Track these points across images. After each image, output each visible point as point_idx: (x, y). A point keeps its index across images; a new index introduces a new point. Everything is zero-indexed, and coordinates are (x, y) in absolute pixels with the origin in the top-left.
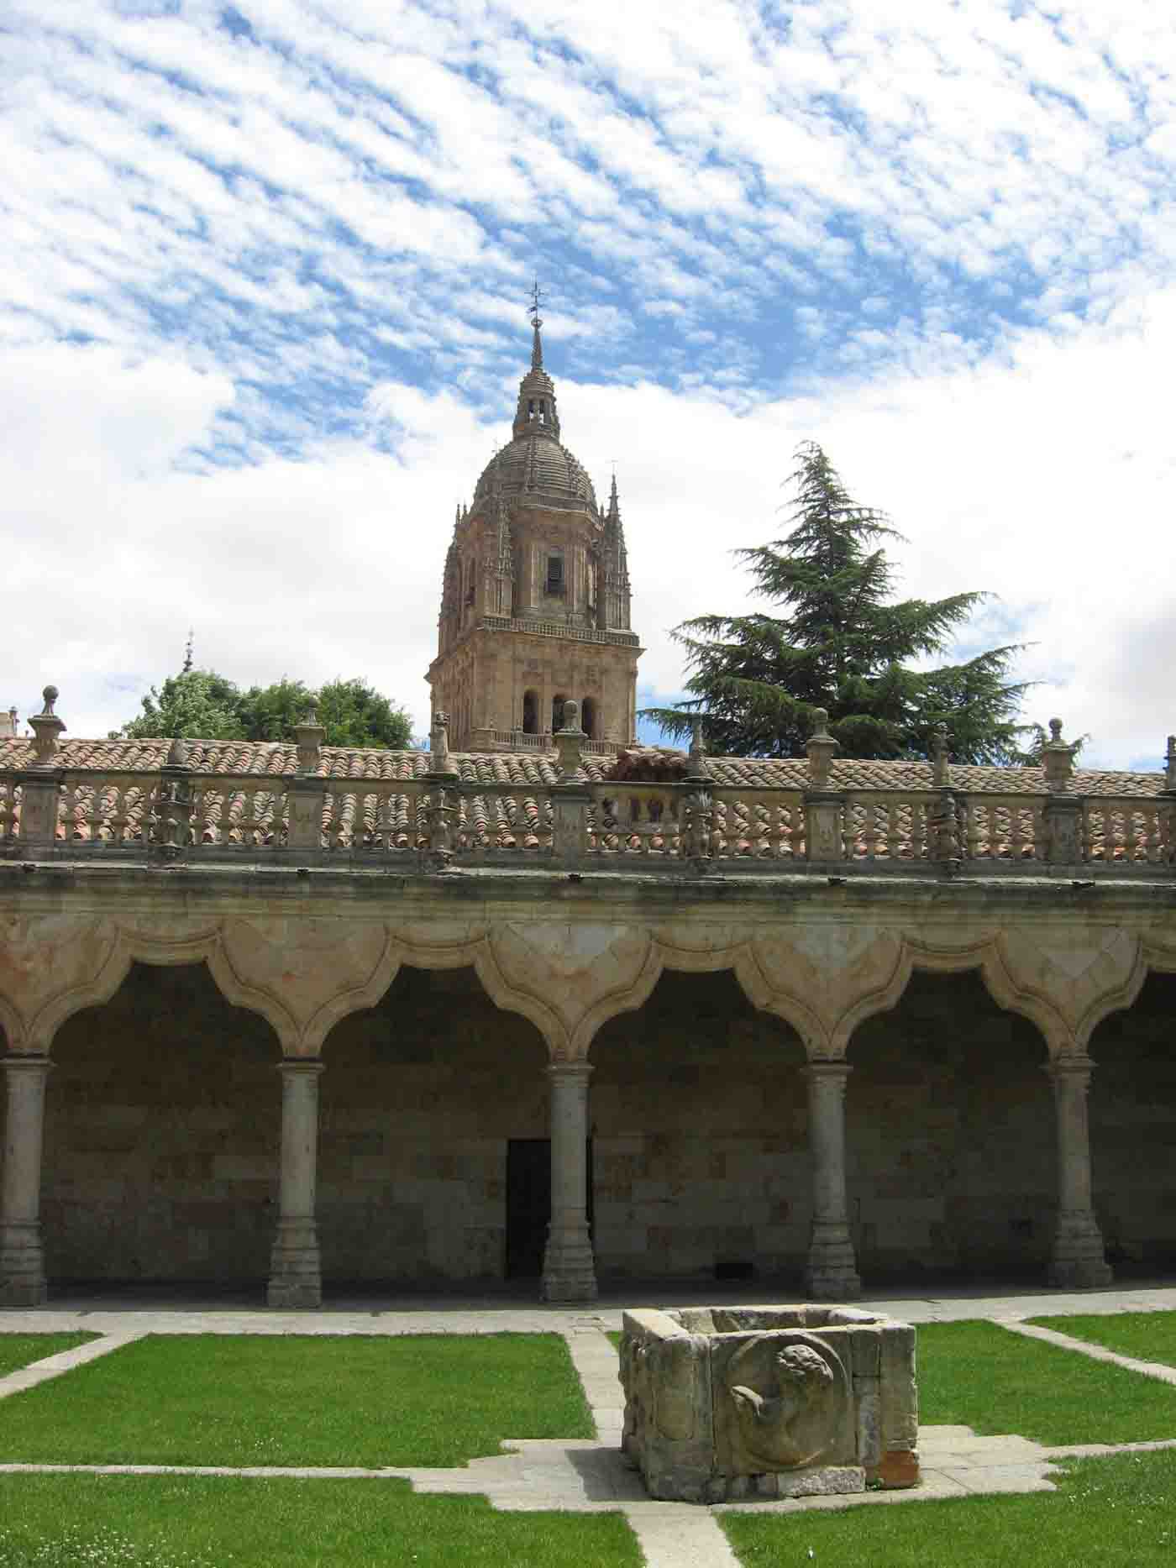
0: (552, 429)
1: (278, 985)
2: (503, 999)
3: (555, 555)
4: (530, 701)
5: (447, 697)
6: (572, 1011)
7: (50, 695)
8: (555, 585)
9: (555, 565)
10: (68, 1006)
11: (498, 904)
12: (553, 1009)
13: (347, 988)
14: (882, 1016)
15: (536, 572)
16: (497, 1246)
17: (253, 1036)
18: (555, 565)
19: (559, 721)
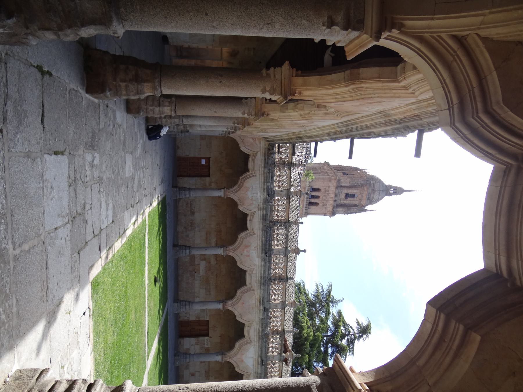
0: (390, 195)
1: (241, 301)
2: (237, 345)
3: (356, 196)
4: (318, 190)
5: (320, 168)
6: (234, 359)
7: (304, 251)
8: (347, 196)
9: (353, 196)
10: (237, 259)
11: (257, 345)
12: (236, 355)
13: (241, 315)
14: (234, 368)
15: (351, 191)
16: (186, 319)
17: (230, 295)
18: (353, 196)
19: (313, 197)
